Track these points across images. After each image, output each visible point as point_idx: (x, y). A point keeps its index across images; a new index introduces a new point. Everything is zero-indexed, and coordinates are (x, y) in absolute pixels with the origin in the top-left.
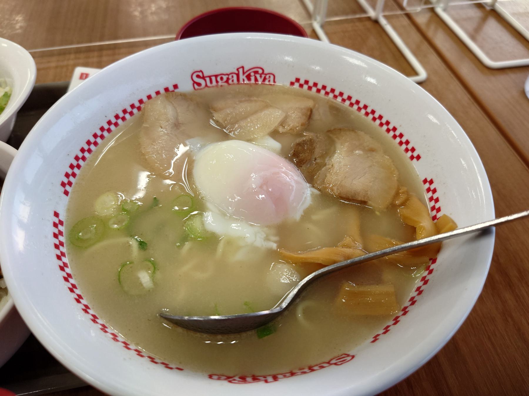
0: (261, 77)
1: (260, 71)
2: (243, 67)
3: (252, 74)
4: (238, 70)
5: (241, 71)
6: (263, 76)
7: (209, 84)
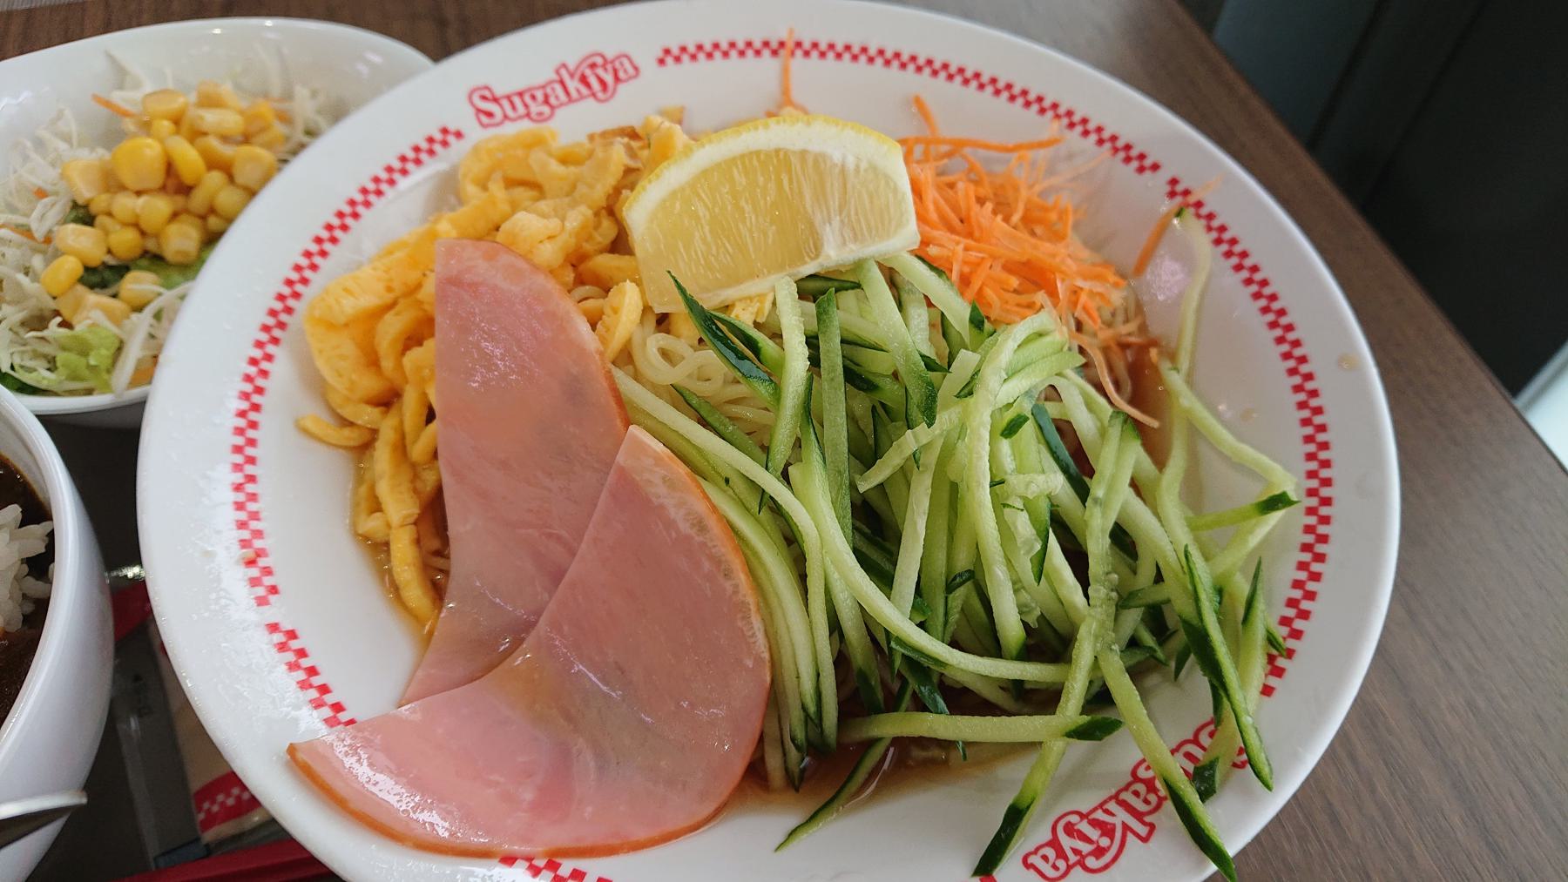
0: (1076, 851)
1: (1091, 862)
3: (1104, 842)
4: (1152, 827)
6: (1073, 858)
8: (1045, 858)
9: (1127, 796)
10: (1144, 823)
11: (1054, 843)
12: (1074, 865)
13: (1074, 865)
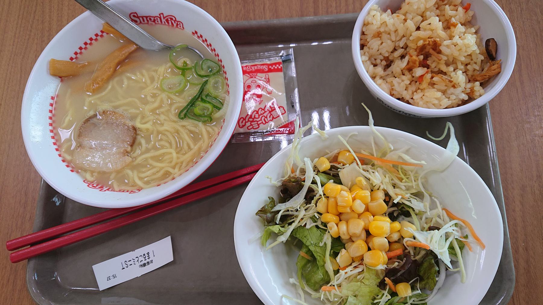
1: (174, 19)
2: (163, 14)
3: (169, 19)
4: (160, 15)
5: (162, 15)
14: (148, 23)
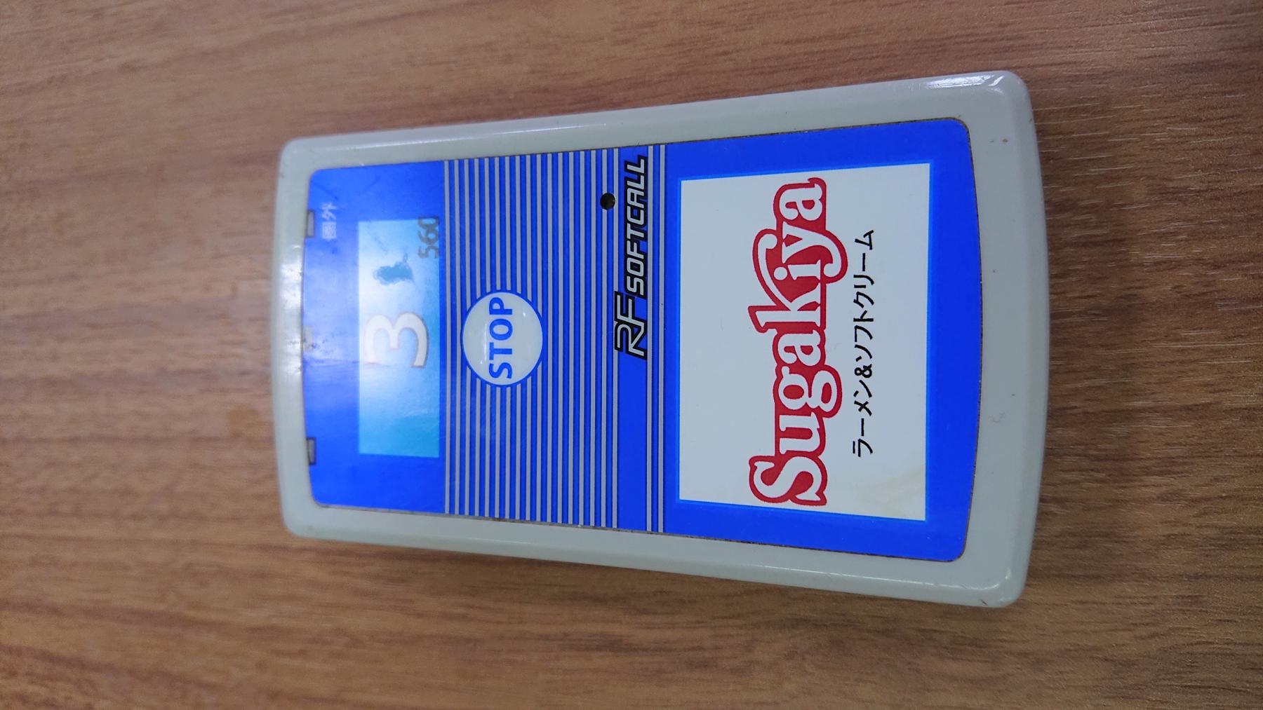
0: (792, 240)
1: (769, 242)
2: (753, 310)
3: (780, 274)
4: (761, 329)
5: (763, 317)
6: (788, 230)
7: (811, 444)
8: (809, 204)
9: (813, 339)
10: (769, 325)
11: (819, 226)
12: (780, 226)
13: (780, 226)
14: (820, 414)
